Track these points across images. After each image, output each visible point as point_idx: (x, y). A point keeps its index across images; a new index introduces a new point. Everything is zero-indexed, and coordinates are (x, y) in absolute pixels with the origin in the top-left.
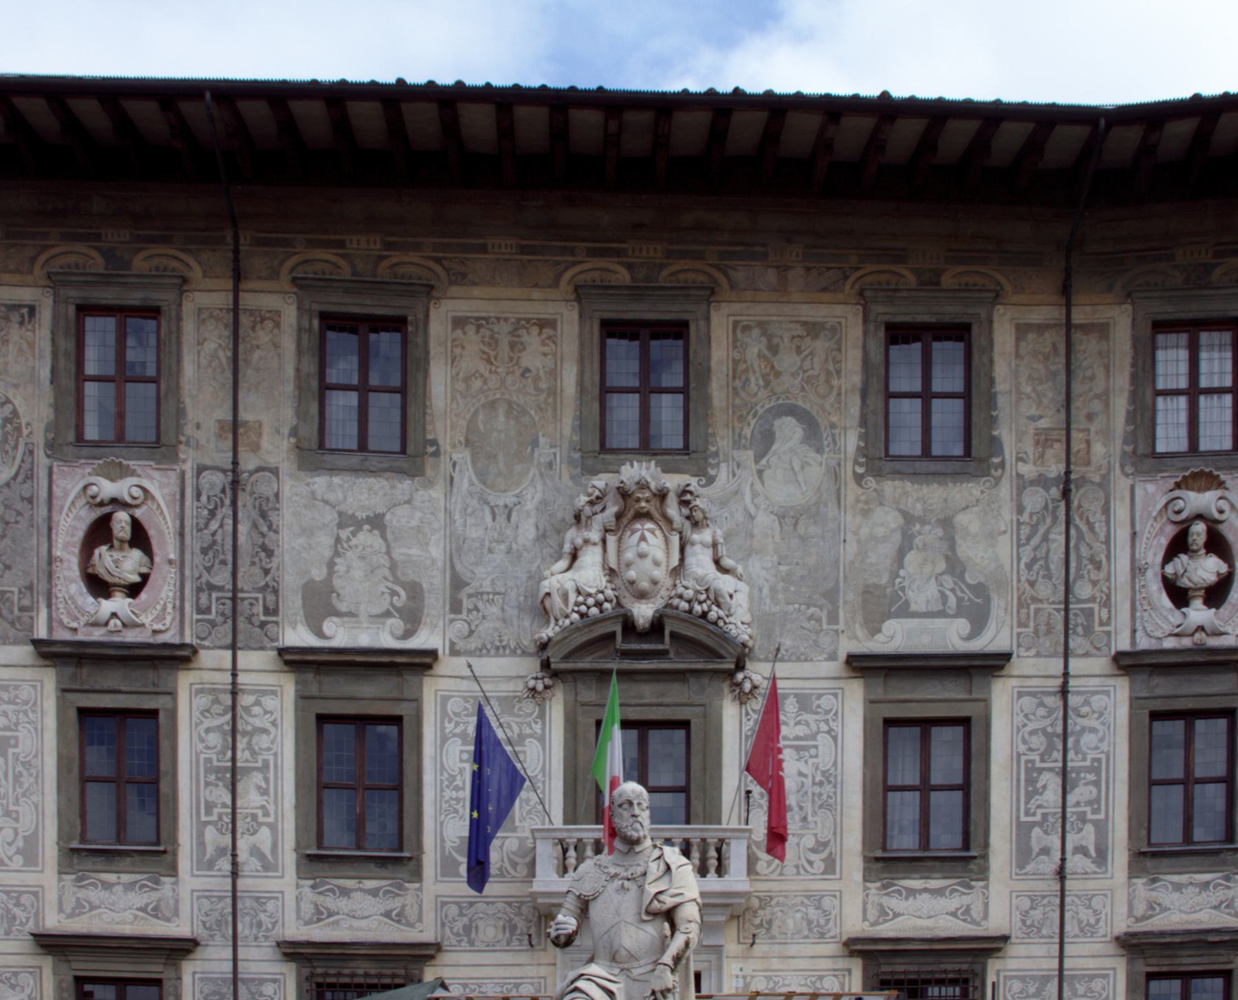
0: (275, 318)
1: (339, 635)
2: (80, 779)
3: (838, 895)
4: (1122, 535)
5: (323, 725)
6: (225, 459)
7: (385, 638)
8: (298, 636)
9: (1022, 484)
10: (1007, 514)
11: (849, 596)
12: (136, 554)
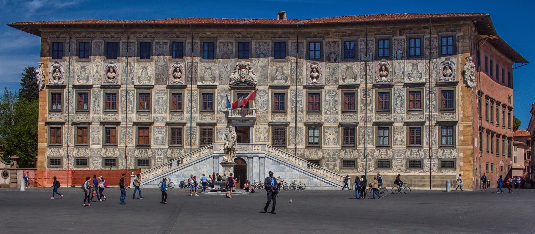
0: (197, 43)
1: (205, 83)
2: (173, 103)
3: (268, 116)
4: (305, 70)
5: (204, 95)
6: (191, 61)
7: (211, 84)
8: (200, 83)
9: (292, 63)
10: (290, 67)
11: (270, 77)
12: (180, 73)
